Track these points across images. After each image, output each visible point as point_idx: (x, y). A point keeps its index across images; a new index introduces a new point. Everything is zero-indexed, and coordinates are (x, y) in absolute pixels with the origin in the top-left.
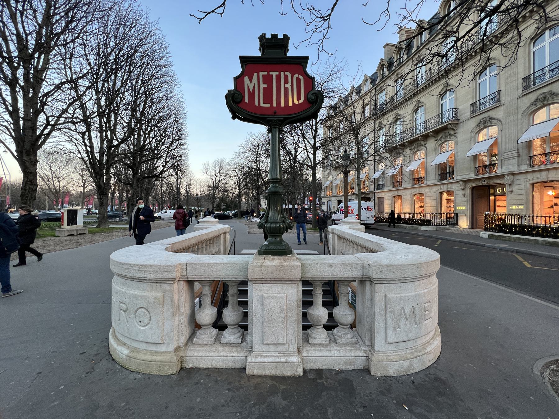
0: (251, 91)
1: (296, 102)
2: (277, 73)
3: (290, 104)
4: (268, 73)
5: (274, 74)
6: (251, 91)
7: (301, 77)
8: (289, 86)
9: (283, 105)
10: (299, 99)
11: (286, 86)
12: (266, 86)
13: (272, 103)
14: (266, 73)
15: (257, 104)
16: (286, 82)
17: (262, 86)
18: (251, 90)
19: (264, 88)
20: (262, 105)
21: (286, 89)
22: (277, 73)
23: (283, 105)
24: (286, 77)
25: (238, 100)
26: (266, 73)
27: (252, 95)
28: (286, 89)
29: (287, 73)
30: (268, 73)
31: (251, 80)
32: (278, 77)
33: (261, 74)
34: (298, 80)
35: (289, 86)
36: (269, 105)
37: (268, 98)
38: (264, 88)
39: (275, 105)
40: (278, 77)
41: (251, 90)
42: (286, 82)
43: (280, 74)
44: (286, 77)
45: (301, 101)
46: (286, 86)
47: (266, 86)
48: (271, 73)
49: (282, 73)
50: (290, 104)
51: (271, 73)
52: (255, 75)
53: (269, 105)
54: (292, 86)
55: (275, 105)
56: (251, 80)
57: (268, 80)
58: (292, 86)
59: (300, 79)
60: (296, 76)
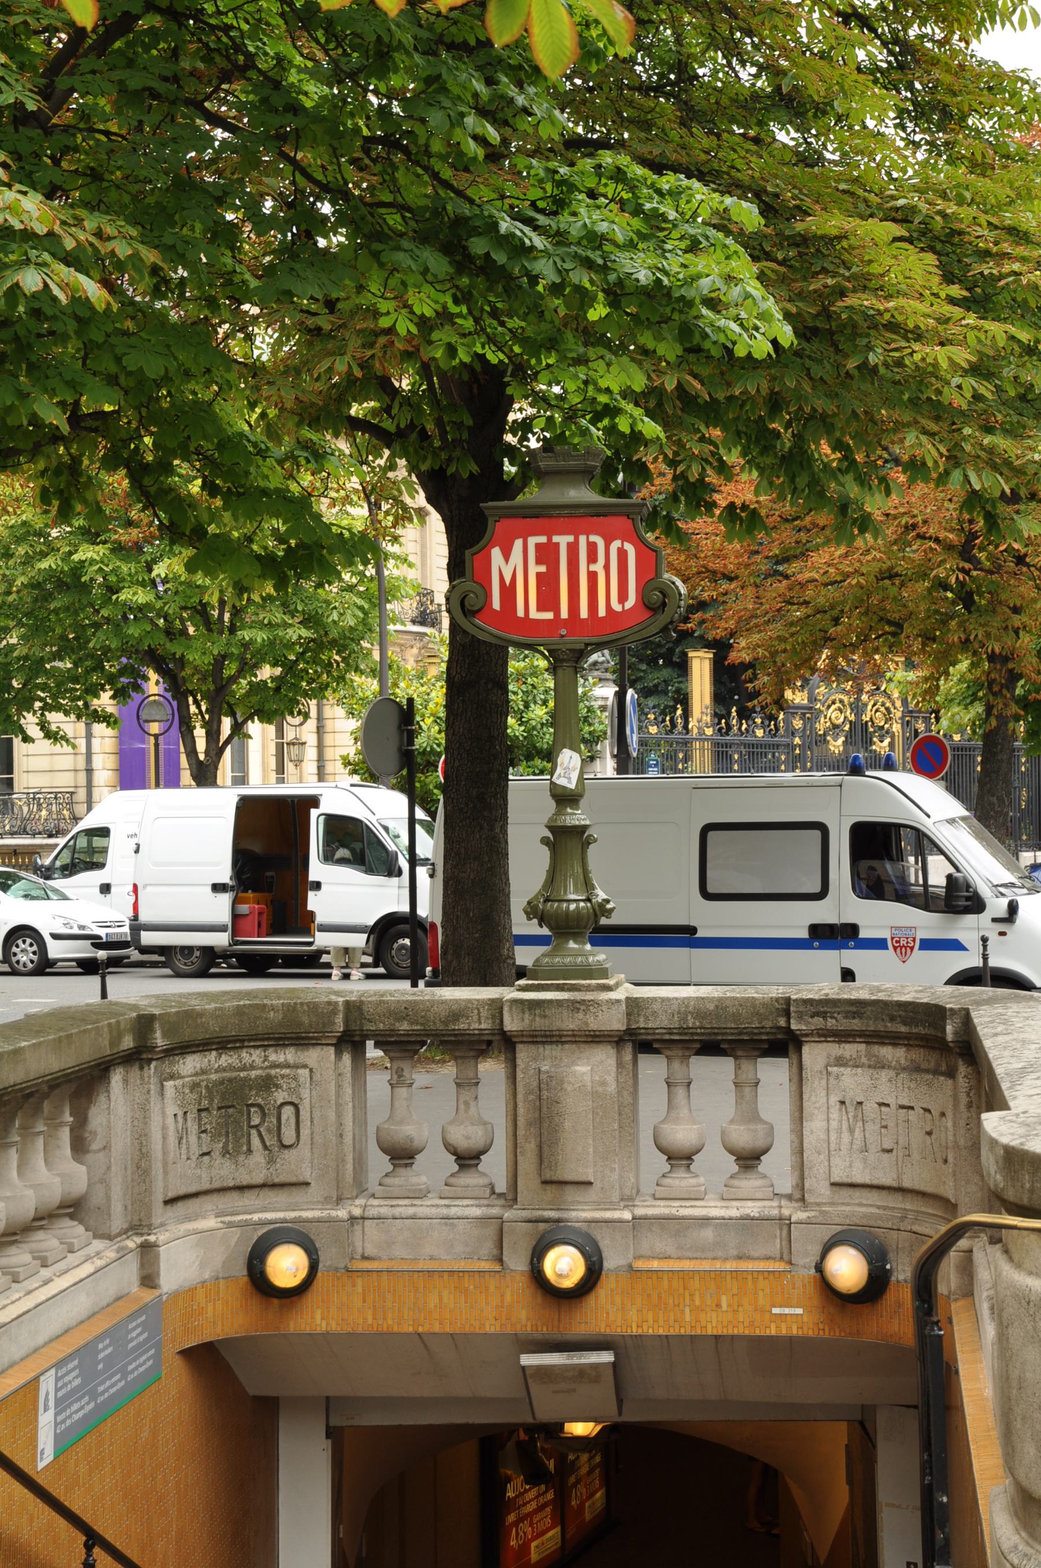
0: (508, 582)
1: (617, 607)
2: (570, 538)
3: (602, 612)
4: (550, 539)
5: (563, 540)
6: (508, 582)
7: (630, 548)
8: (598, 567)
9: (584, 613)
10: (623, 597)
11: (593, 568)
12: (543, 569)
13: (557, 613)
14: (543, 539)
15: (521, 613)
16: (592, 558)
17: (534, 569)
18: (508, 581)
19: (538, 575)
20: (534, 614)
21: (592, 577)
22: (570, 538)
23: (584, 613)
24: (592, 548)
25: (475, 608)
26: (543, 539)
27: (508, 592)
28: (592, 577)
29: (593, 538)
30: (550, 539)
31: (507, 558)
32: (573, 548)
33: (533, 541)
34: (622, 554)
35: (598, 567)
36: (549, 615)
37: (548, 599)
38: (538, 575)
39: (564, 614)
40: (573, 548)
41: (508, 581)
42: (592, 558)
43: (577, 540)
44: (592, 548)
45: (630, 603)
46: (593, 568)
47: (543, 569)
48: (556, 539)
49: (583, 539)
50: (602, 612)
51: (556, 539)
52: (518, 543)
53: (549, 615)
54: (607, 567)
55: (564, 614)
56: (507, 558)
57: (547, 554)
58: (607, 567)
59: (626, 552)
60: (616, 544)
